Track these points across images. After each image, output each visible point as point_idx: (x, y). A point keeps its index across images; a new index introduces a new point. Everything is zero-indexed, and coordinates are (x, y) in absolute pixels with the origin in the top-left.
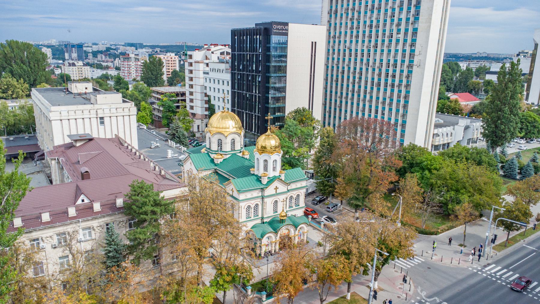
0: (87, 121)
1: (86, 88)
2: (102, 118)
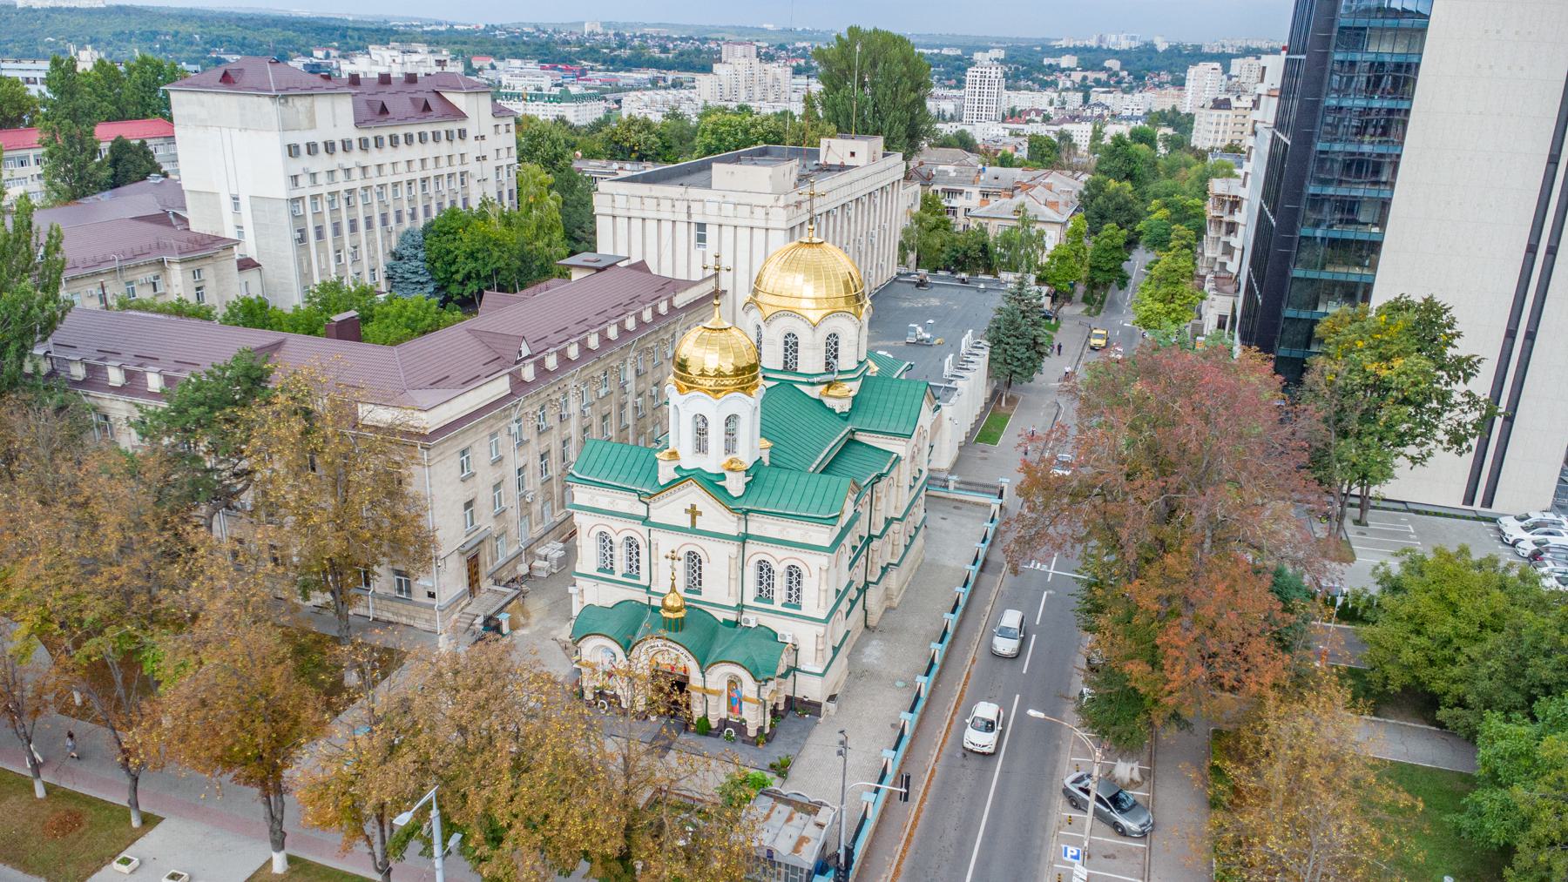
0: (666, 226)
1: (853, 154)
2: (702, 227)
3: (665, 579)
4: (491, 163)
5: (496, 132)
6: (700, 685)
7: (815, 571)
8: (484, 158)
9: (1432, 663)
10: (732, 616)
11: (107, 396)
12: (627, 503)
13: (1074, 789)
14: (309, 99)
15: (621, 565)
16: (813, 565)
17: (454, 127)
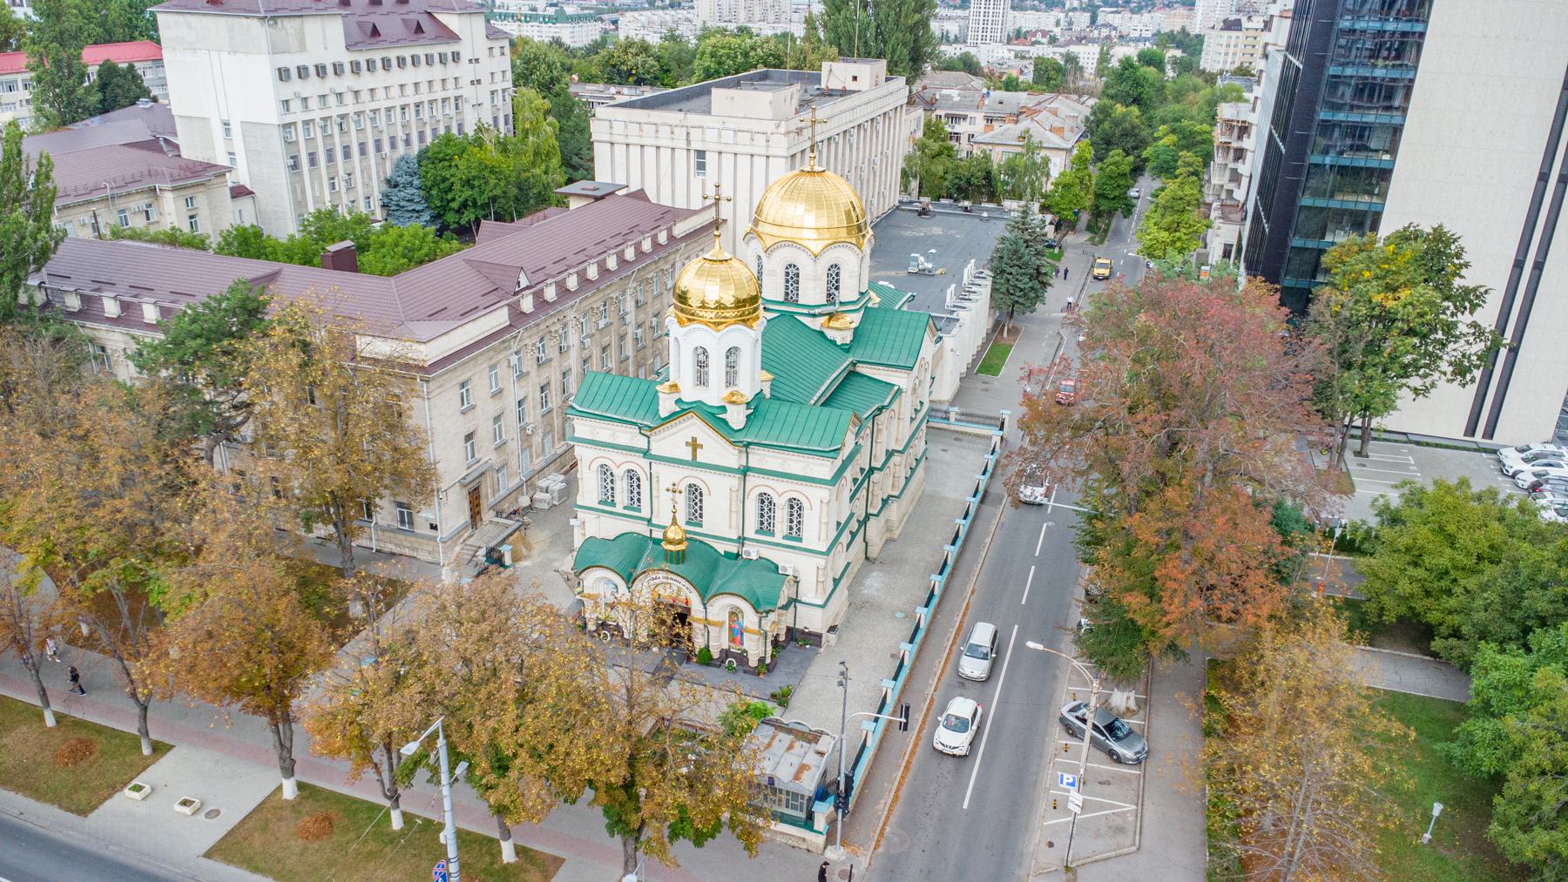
0: (665, 154)
1: (855, 78)
2: (701, 154)
3: (665, 512)
4: (486, 87)
5: (491, 55)
6: (702, 616)
7: (816, 505)
8: (479, 81)
9: (1428, 594)
10: (733, 549)
11: (103, 327)
12: (627, 436)
13: (1071, 717)
14: (299, 20)
15: (622, 498)
16: (814, 497)
17: (448, 49)
